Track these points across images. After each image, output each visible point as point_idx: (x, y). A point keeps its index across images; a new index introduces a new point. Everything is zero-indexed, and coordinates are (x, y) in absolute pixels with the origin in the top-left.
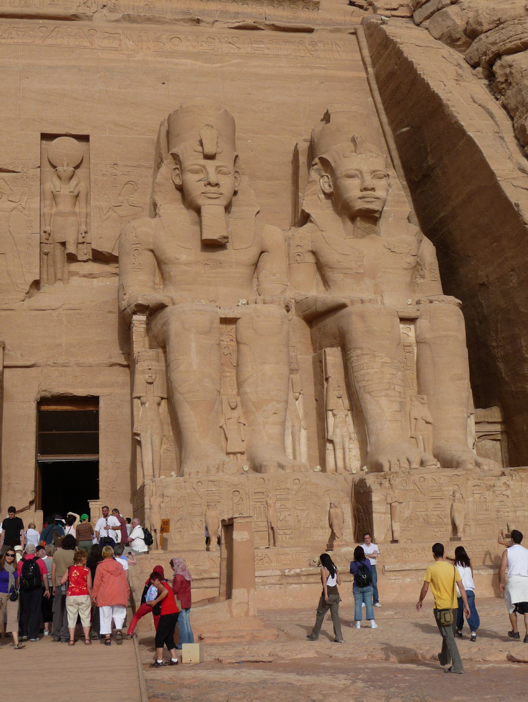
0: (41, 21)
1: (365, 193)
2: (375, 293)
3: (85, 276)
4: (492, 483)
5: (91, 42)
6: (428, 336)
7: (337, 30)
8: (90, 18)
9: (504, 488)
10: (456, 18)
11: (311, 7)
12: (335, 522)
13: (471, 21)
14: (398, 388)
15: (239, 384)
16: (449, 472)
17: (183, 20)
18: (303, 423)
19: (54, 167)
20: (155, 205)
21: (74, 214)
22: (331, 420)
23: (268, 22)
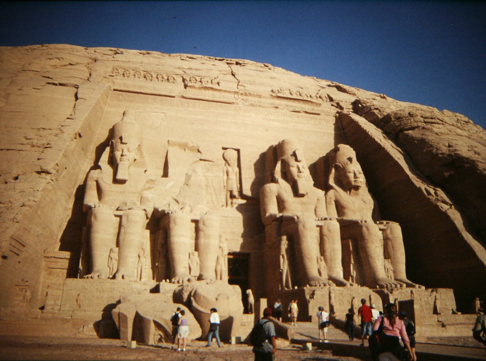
6: (390, 236)
8: (238, 104)
11: (318, 106)
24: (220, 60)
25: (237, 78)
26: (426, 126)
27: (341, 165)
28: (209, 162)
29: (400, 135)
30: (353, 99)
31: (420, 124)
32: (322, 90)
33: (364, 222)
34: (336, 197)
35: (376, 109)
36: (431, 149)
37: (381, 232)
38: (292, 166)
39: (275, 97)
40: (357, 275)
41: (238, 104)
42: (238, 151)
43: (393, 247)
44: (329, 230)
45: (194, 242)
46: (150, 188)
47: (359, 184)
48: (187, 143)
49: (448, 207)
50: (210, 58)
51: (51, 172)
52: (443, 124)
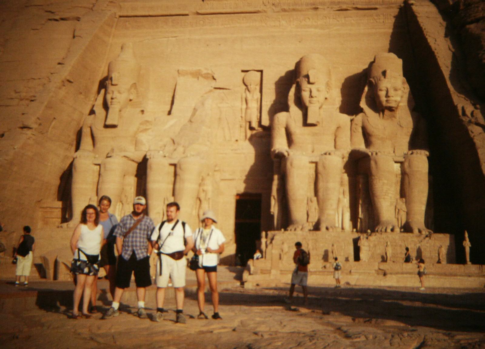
0: (243, 15)
1: (388, 99)
5: (266, 24)
6: (407, 170)
8: (265, 12)
18: (349, 210)
23: (354, 6)
27: (374, 81)
28: (224, 91)
33: (374, 154)
34: (363, 123)
37: (399, 165)
38: (304, 91)
40: (365, 217)
41: (265, 12)
42: (261, 71)
43: (409, 183)
44: (324, 167)
45: (171, 186)
46: (146, 130)
48: (200, 70)
51: (31, 127)
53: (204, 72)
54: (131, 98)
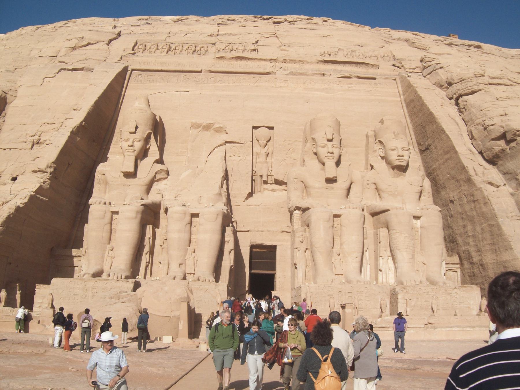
2: (402, 203)
3: (271, 190)
4: (450, 292)
7: (387, 78)
9: (455, 294)
10: (443, 76)
11: (375, 67)
12: (383, 306)
13: (449, 78)
14: (411, 248)
15: (341, 244)
16: (432, 287)
17: (316, 74)
19: (258, 141)
20: (304, 161)
21: (267, 162)
22: (381, 261)
23: (355, 75)
24: (268, 19)
25: (281, 40)
26: (487, 90)
29: (459, 101)
30: (421, 54)
31: (480, 87)
32: (387, 46)
35: (441, 68)
36: (484, 119)
39: (322, 61)
42: (271, 128)
47: (404, 164)
49: (496, 189)
50: (256, 17)
52: (511, 85)
53: (217, 126)
54: (148, 147)
